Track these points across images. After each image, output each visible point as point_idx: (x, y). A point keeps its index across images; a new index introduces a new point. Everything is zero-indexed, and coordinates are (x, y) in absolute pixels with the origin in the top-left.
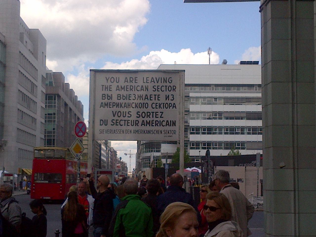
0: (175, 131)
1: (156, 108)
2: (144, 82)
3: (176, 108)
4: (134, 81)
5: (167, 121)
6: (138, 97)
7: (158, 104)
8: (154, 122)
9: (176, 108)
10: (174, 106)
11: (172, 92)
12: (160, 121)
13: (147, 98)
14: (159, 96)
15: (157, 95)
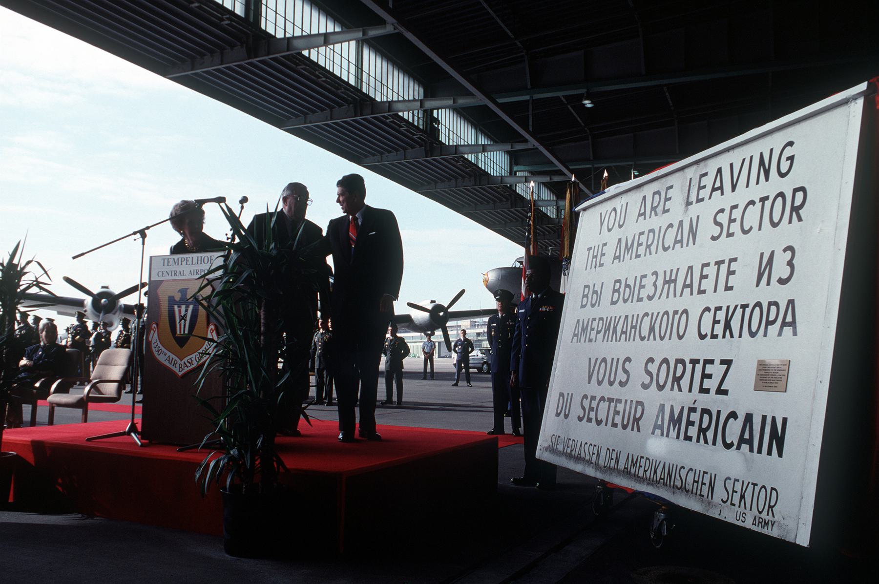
0: (774, 492)
1: (714, 336)
2: (690, 200)
3: (795, 334)
4: (660, 209)
5: (749, 418)
6: (665, 282)
7: (721, 316)
8: (695, 417)
9: (795, 334)
10: (789, 319)
11: (789, 232)
12: (719, 412)
13: (691, 286)
14: (734, 266)
15: (712, 264)
